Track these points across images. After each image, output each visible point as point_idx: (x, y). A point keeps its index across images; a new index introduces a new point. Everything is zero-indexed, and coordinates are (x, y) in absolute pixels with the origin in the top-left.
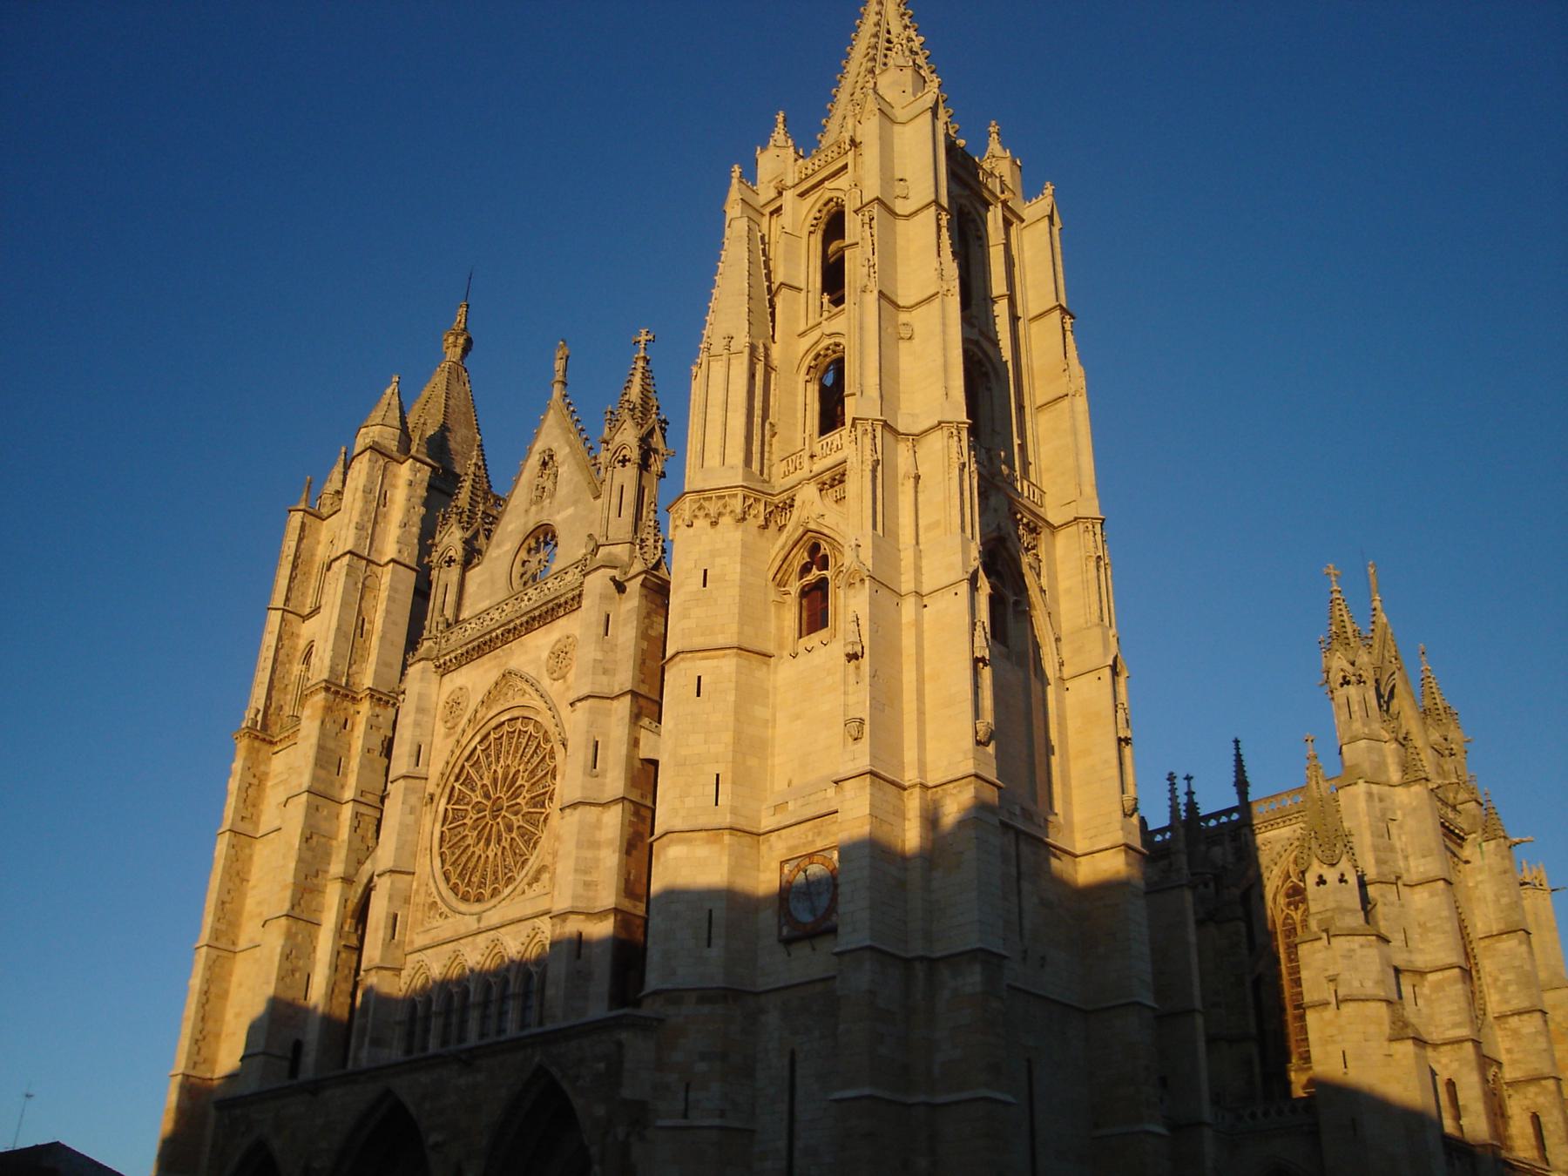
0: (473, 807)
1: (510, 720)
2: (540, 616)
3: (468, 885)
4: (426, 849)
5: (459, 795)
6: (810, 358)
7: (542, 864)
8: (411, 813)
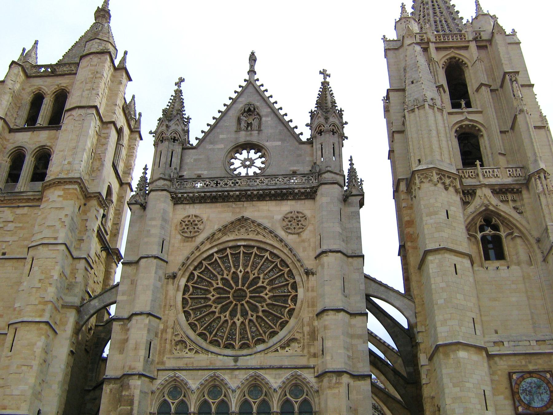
0: (214, 290)
1: (244, 246)
2: (273, 195)
3: (215, 336)
4: (171, 306)
5: (197, 279)
6: (457, 126)
7: (292, 337)
8: (159, 281)
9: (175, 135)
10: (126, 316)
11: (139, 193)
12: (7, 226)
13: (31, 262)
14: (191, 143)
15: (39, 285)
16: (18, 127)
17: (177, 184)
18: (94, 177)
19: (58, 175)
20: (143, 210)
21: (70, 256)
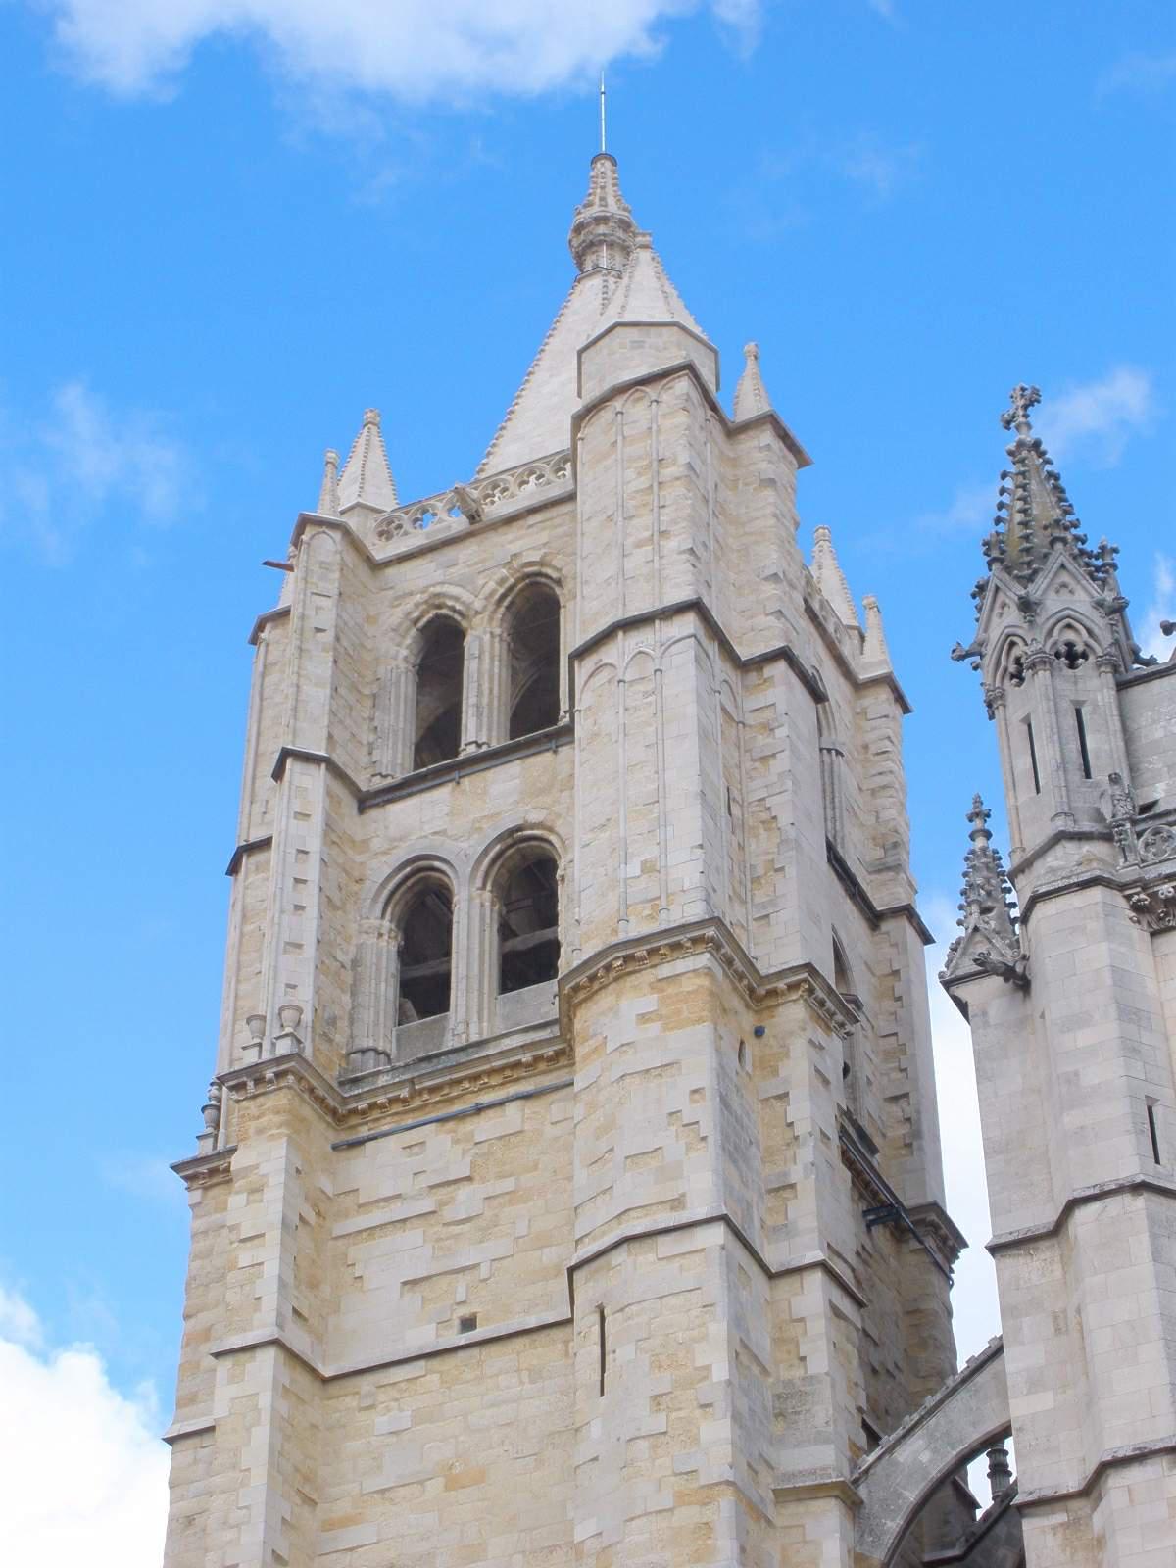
9: (1070, 636)
10: (1072, 1483)
11: (982, 926)
12: (450, 1201)
13: (596, 1328)
14: (1144, 655)
15: (660, 1422)
16: (389, 781)
17: (1140, 843)
18: (764, 905)
19: (615, 931)
20: (1021, 994)
21: (753, 1269)
